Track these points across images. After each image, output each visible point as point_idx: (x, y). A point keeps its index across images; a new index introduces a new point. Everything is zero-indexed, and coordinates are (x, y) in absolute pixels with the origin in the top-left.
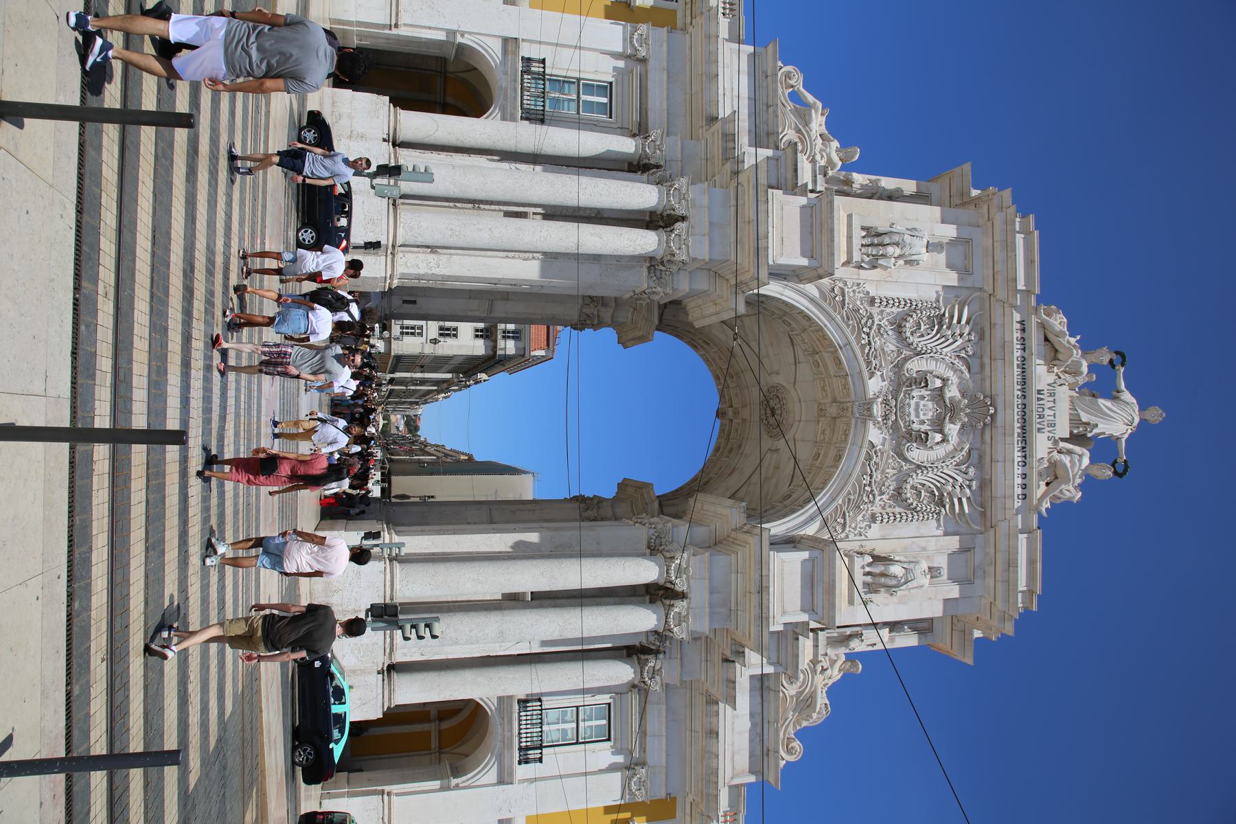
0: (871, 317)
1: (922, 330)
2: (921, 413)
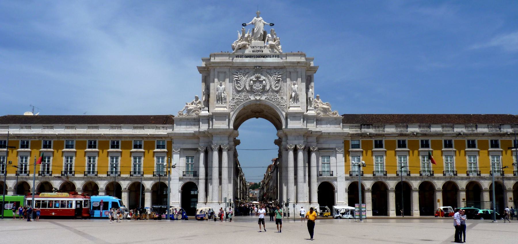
0: (237, 99)
1: (239, 85)
2: (258, 86)
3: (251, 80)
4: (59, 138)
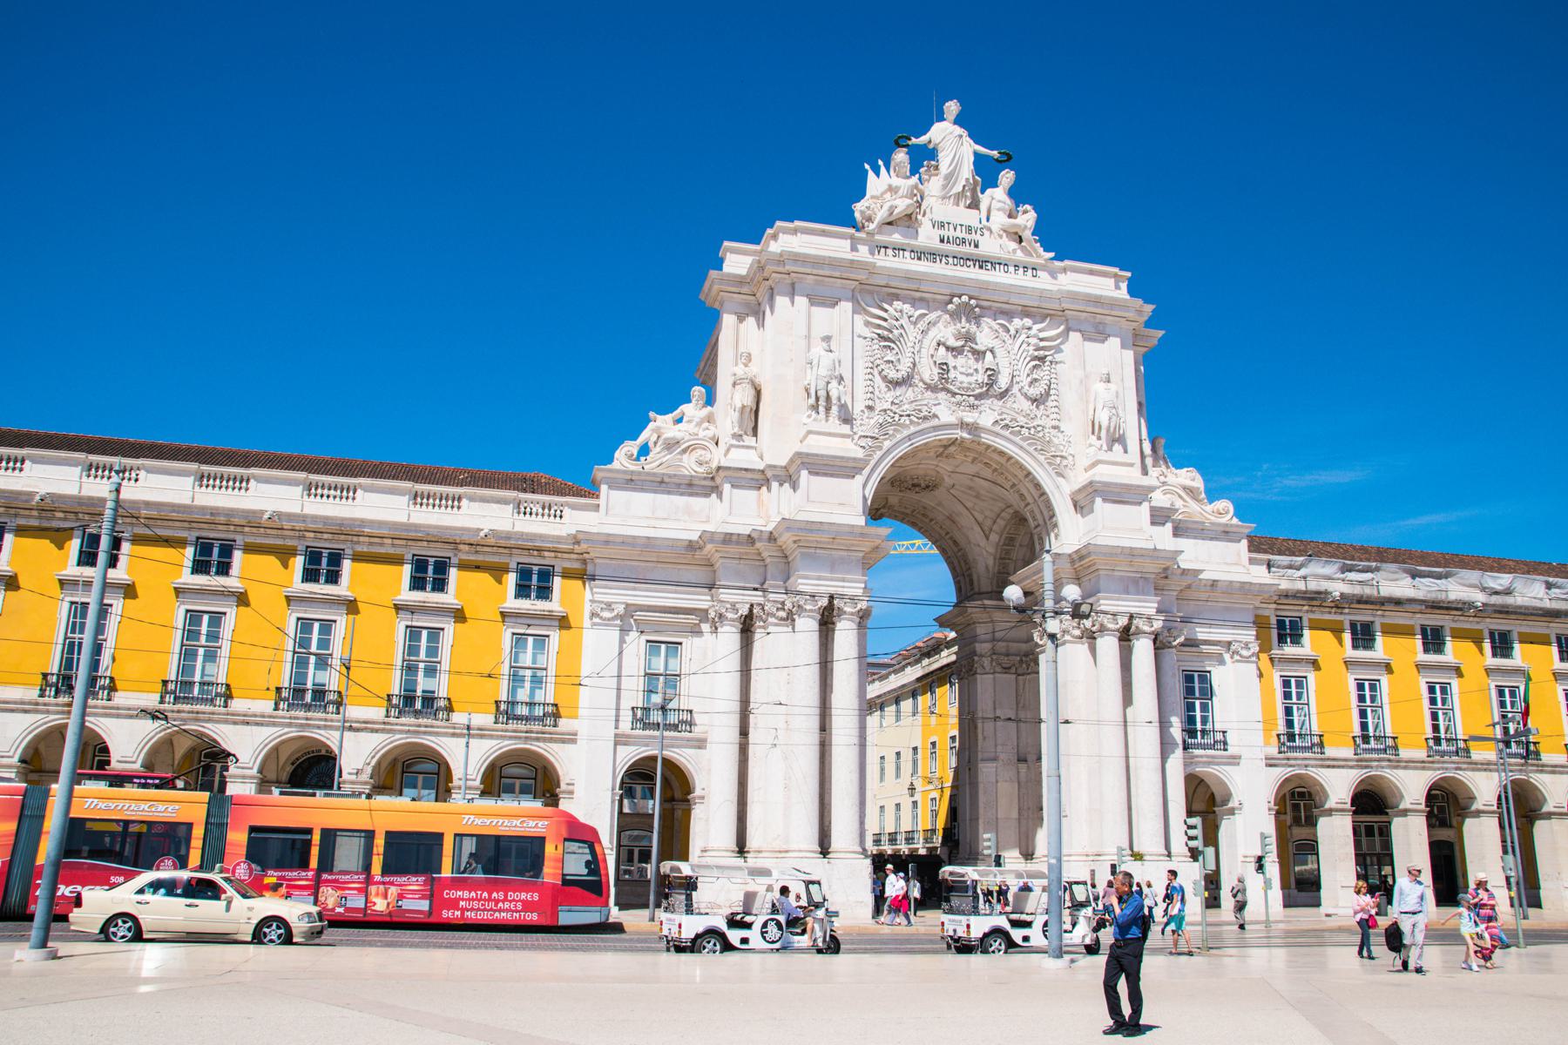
0: (885, 411)
2: (971, 371)
3: (939, 345)
4: (49, 514)
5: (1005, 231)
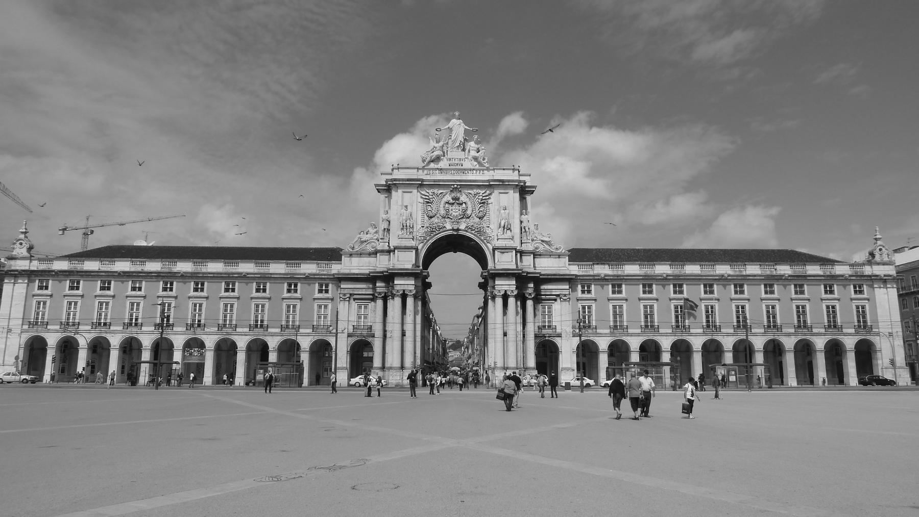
2: (457, 211)
5: (473, 158)
